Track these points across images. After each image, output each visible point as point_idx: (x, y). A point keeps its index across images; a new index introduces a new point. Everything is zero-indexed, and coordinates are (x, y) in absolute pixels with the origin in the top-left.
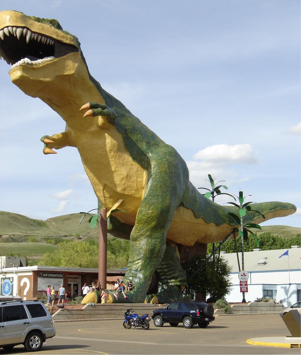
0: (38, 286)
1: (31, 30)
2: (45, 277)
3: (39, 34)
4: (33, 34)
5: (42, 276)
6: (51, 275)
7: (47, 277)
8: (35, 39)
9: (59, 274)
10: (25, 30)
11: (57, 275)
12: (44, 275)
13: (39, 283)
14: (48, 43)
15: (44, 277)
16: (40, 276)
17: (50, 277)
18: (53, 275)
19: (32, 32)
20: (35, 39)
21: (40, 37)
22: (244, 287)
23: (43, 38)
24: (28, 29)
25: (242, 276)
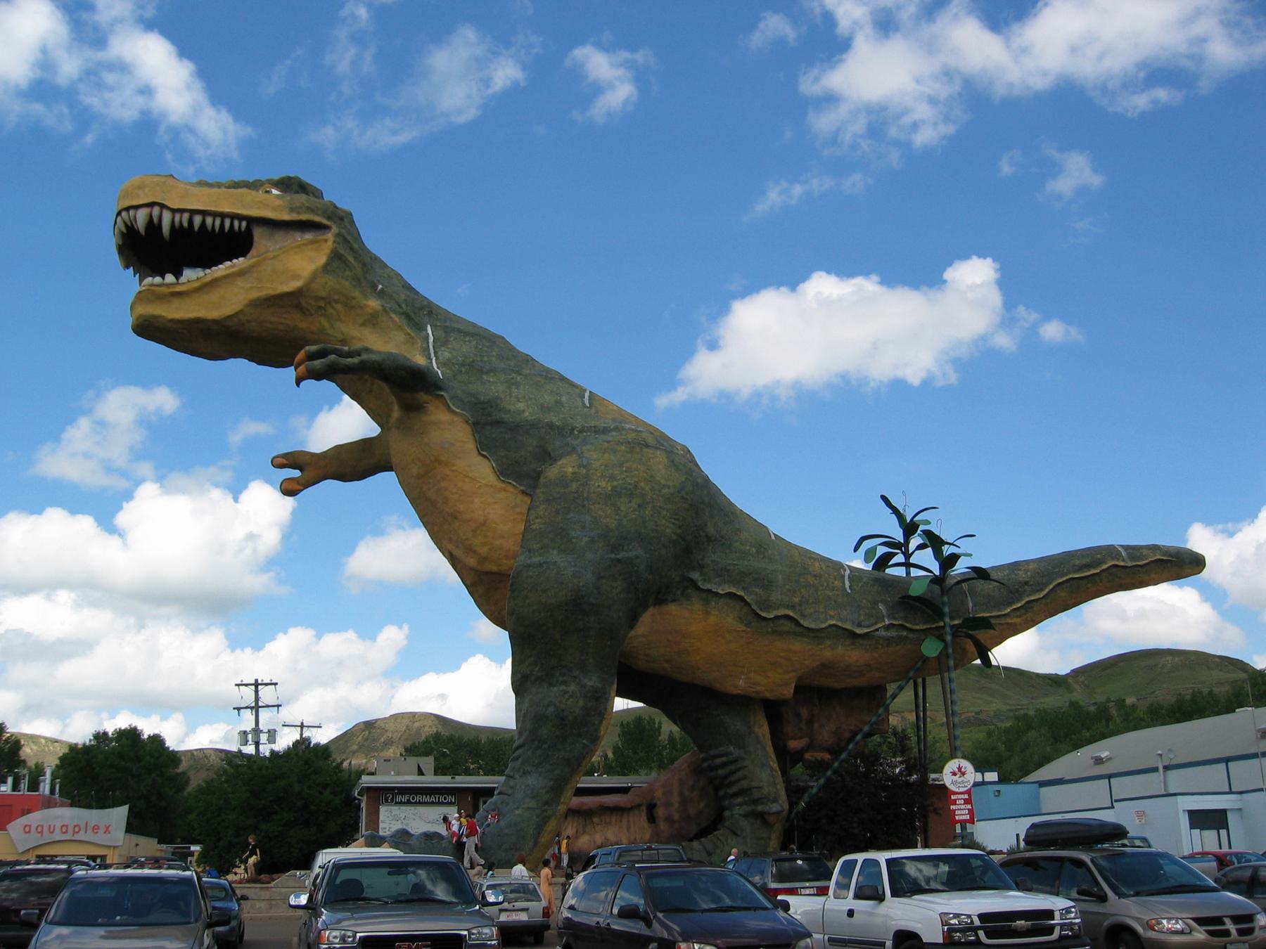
0: (381, 825)
1: (168, 208)
2: (401, 803)
3: (193, 212)
4: (177, 217)
5: (392, 801)
6: (417, 798)
7: (408, 803)
8: (185, 224)
9: (442, 794)
10: (156, 210)
11: (437, 796)
12: (399, 798)
13: (381, 818)
14: (226, 230)
15: (396, 803)
16: (387, 801)
17: (416, 803)
18: (425, 799)
19: (174, 211)
20: (185, 224)
21: (197, 220)
22: (963, 807)
23: (209, 221)
24: (162, 206)
25: (954, 774)
